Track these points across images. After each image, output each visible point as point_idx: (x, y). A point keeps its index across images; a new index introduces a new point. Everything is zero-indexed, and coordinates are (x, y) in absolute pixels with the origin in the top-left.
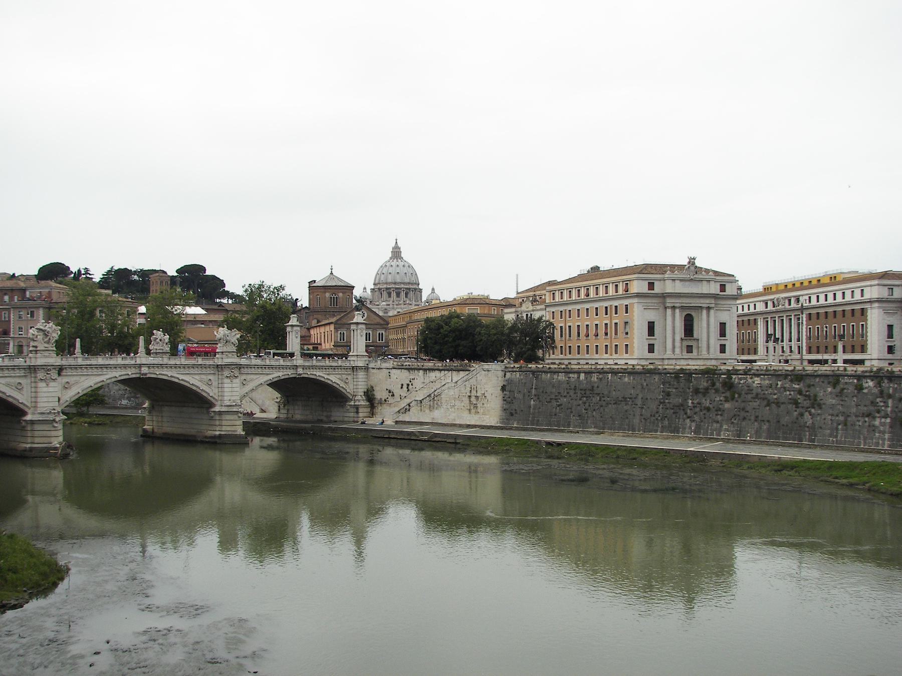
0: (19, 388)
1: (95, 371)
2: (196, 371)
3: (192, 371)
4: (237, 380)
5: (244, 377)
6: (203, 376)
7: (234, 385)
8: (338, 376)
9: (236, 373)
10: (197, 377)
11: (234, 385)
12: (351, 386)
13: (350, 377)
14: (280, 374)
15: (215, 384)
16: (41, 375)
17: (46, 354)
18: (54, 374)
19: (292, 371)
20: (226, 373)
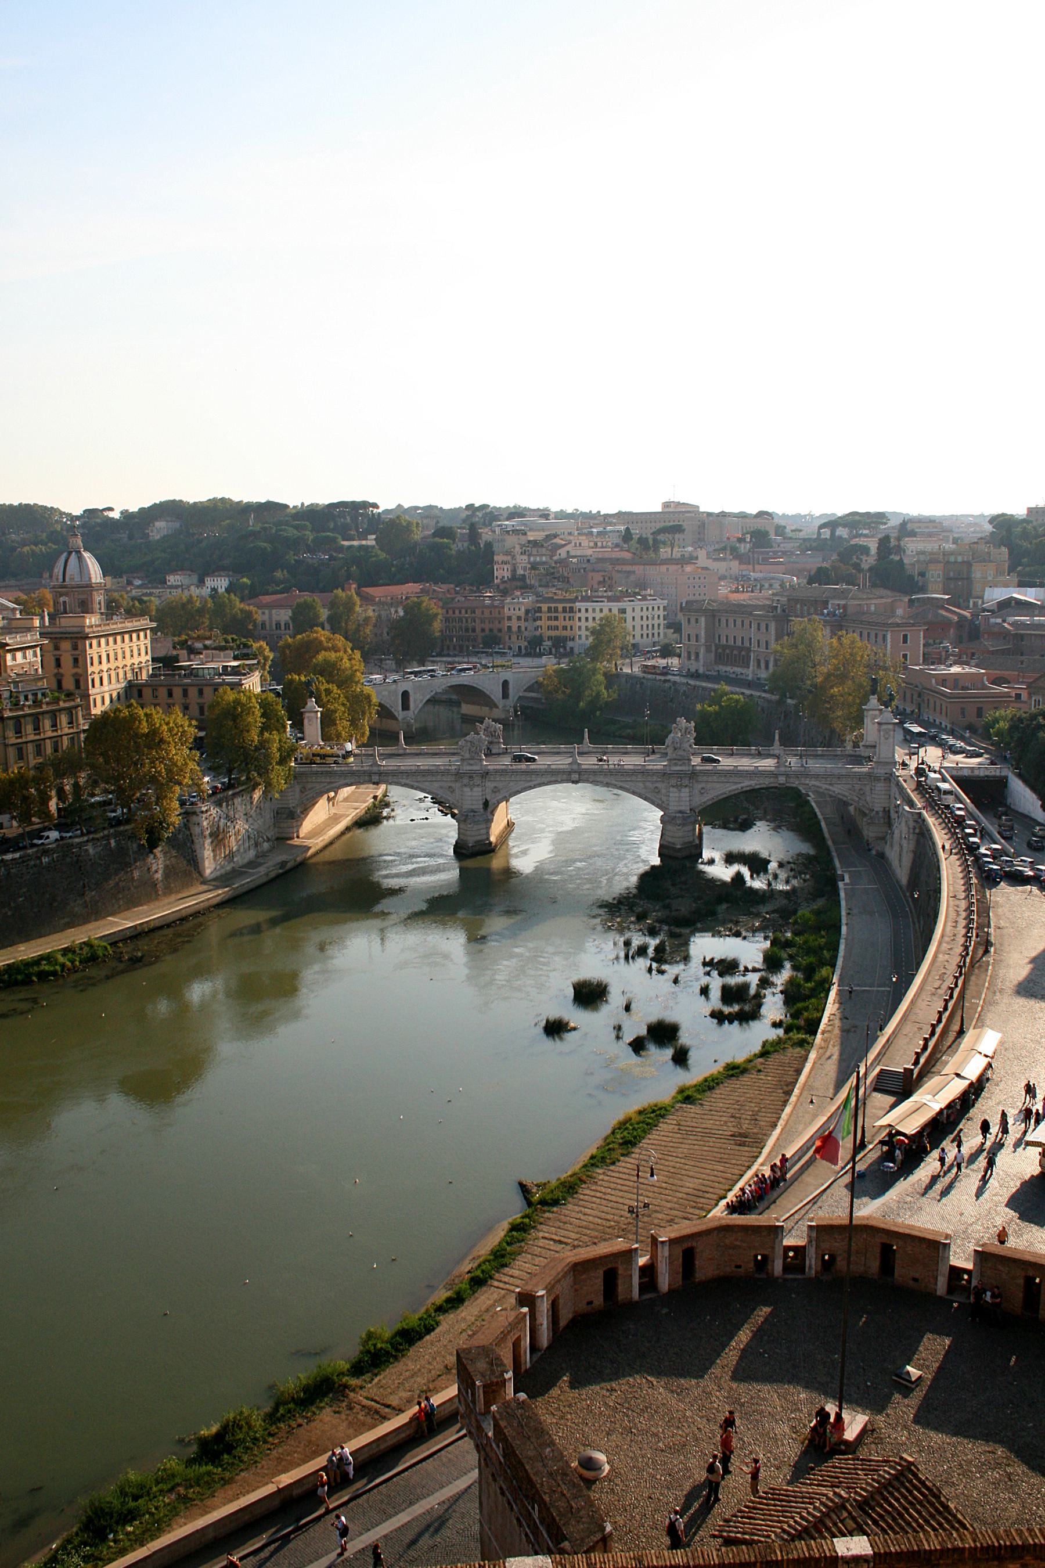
0: (452, 790)
1: (523, 778)
2: (640, 778)
3: (634, 778)
4: (687, 790)
5: (703, 785)
6: (649, 784)
7: (682, 795)
8: (847, 786)
9: (686, 782)
10: (641, 785)
11: (682, 795)
12: (868, 798)
13: (868, 788)
14: (753, 783)
15: (663, 791)
16: (466, 781)
17: (471, 762)
18: (477, 780)
19: (772, 780)
20: (673, 782)
